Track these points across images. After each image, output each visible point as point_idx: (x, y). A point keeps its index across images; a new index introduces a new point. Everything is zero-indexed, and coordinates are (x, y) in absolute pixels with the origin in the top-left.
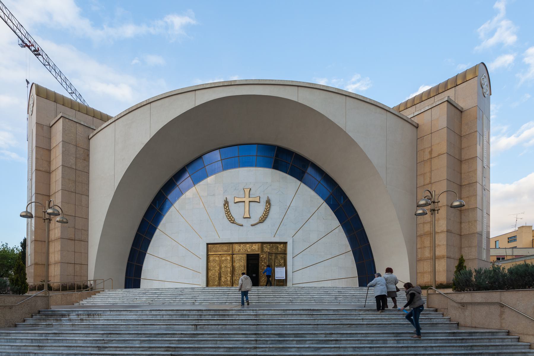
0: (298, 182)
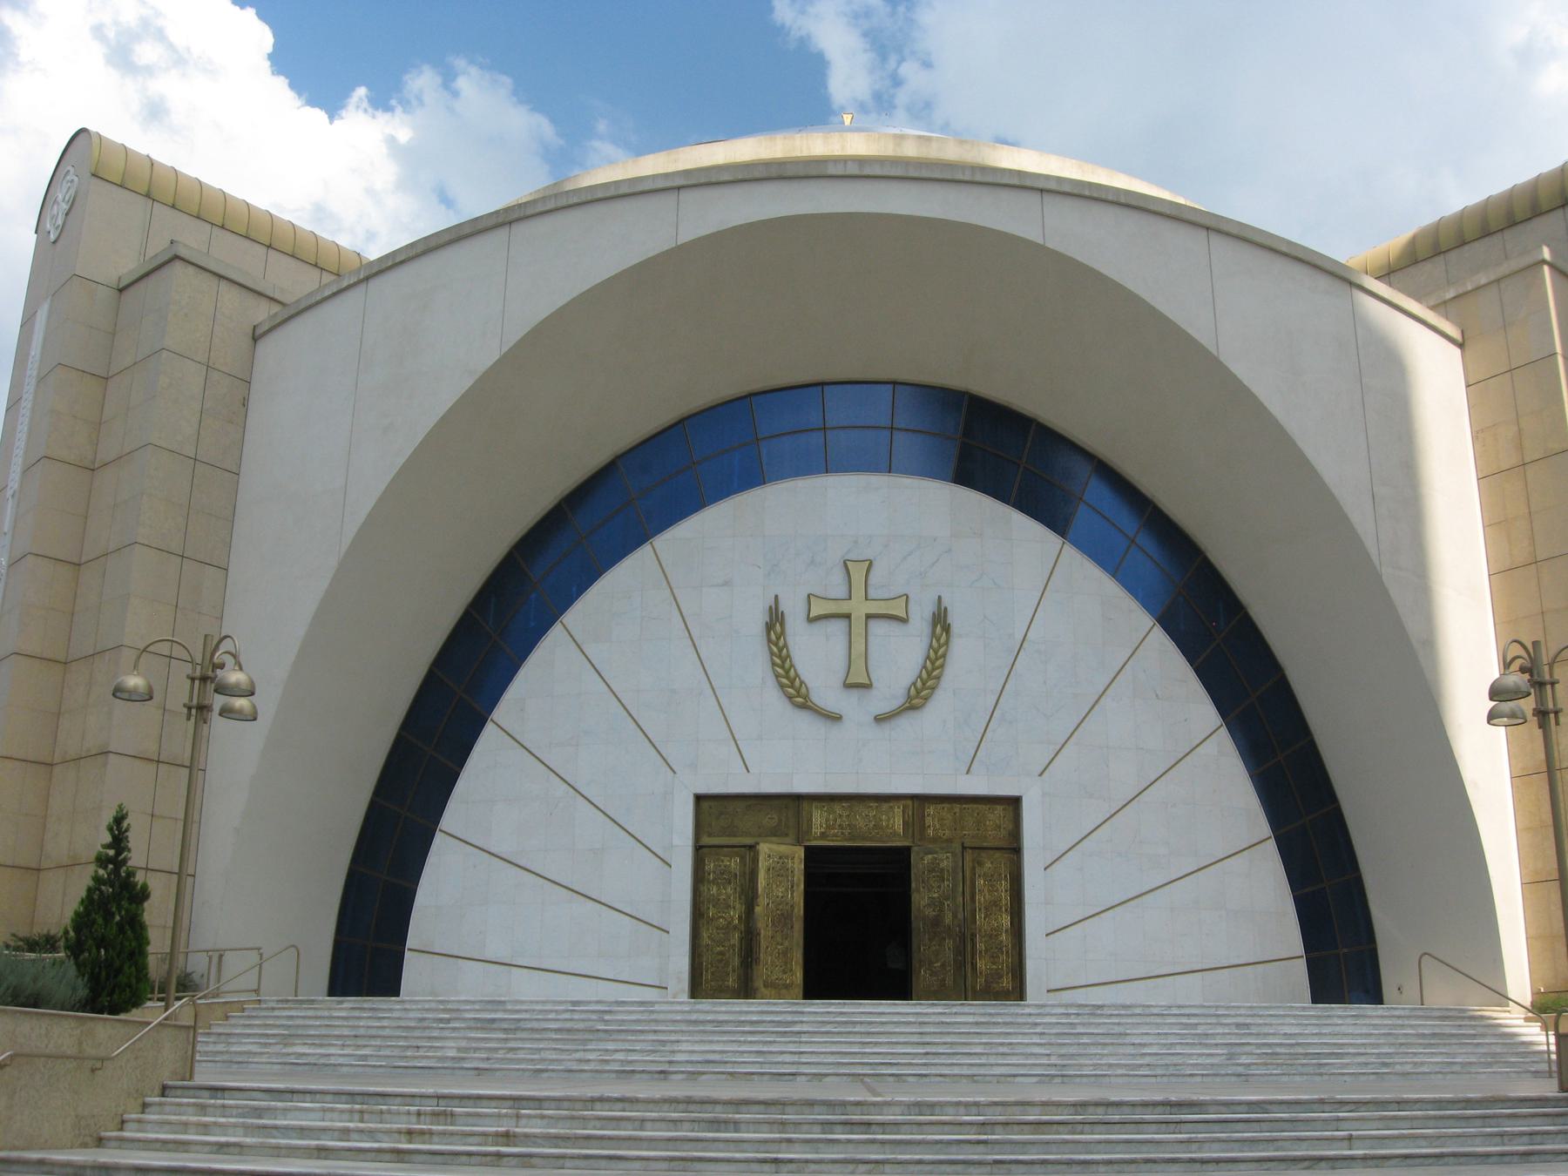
0: (1052, 540)
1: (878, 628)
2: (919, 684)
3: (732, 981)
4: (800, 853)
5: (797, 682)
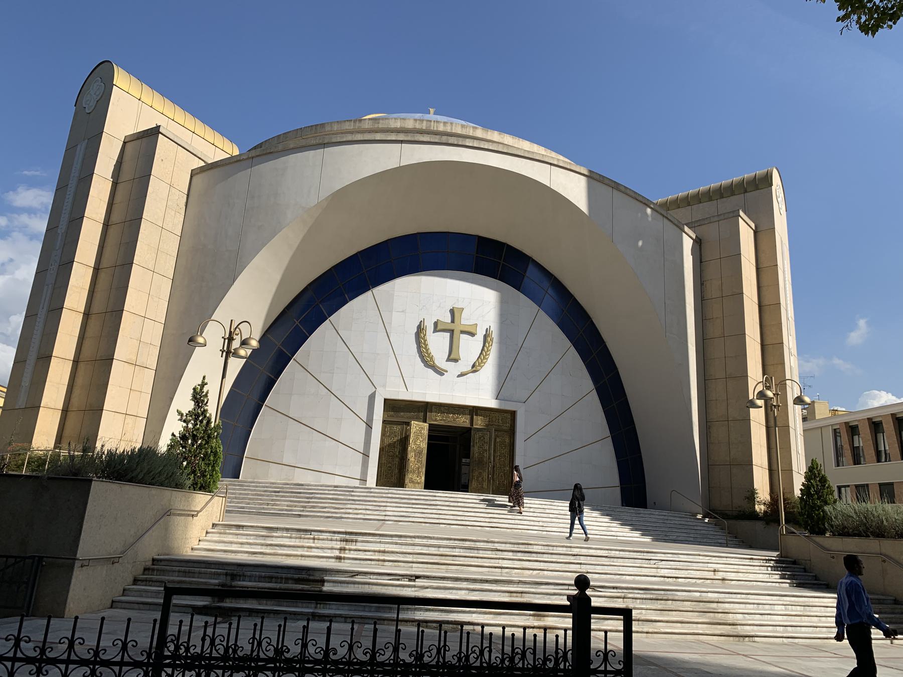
1: (463, 336)
3: (394, 479)
4: (426, 425)
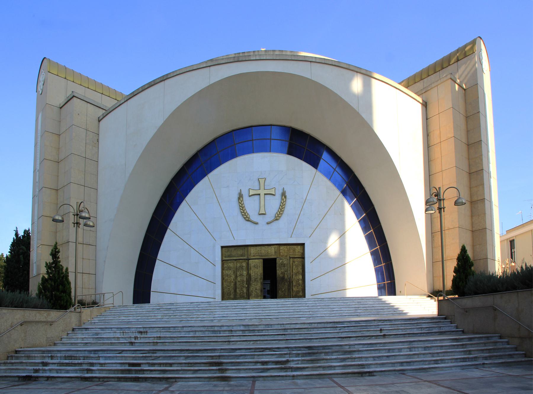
2: (278, 213)
5: (246, 214)
